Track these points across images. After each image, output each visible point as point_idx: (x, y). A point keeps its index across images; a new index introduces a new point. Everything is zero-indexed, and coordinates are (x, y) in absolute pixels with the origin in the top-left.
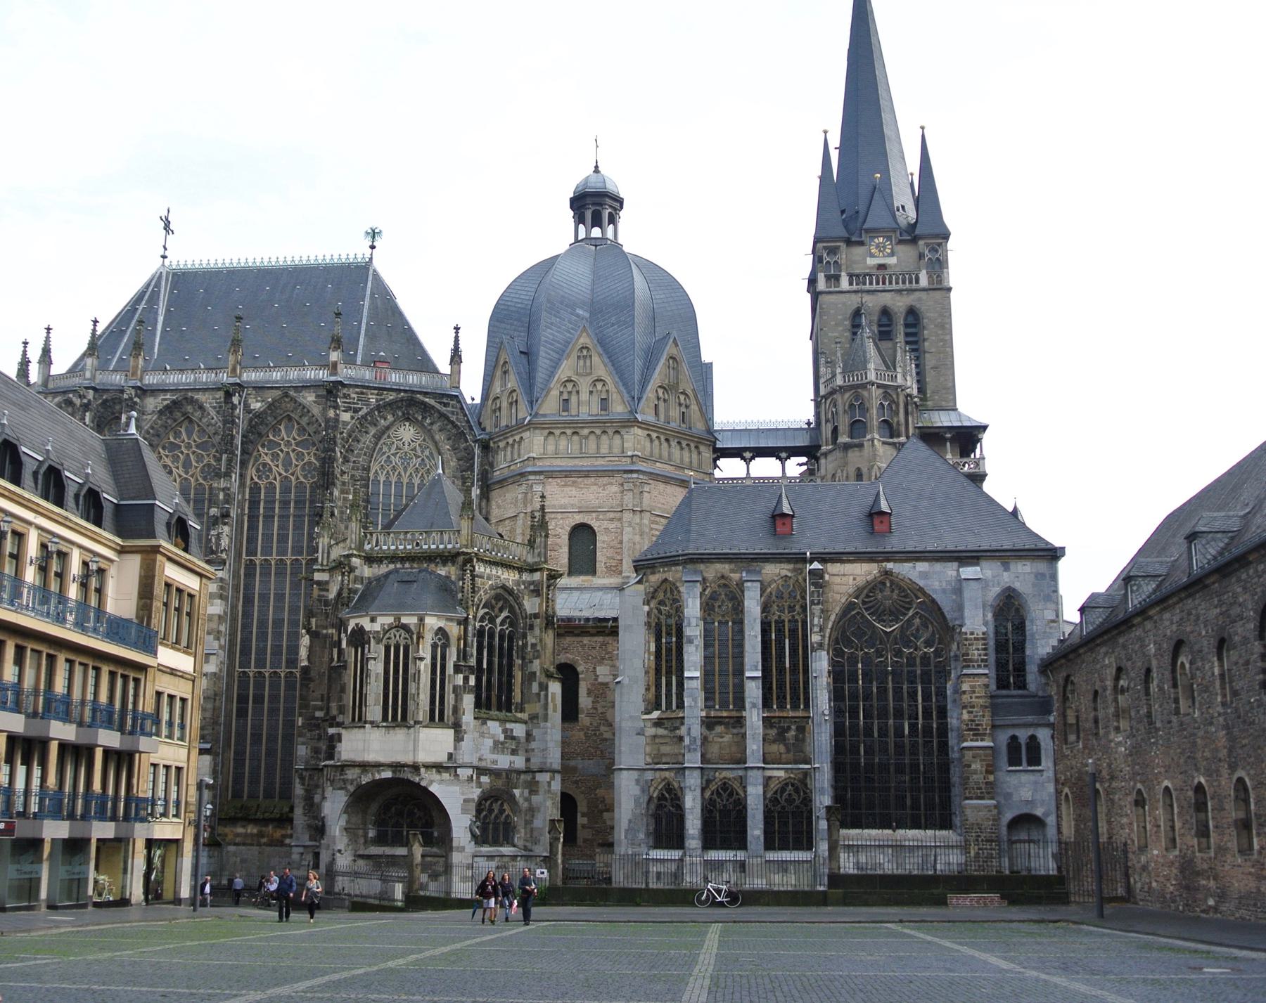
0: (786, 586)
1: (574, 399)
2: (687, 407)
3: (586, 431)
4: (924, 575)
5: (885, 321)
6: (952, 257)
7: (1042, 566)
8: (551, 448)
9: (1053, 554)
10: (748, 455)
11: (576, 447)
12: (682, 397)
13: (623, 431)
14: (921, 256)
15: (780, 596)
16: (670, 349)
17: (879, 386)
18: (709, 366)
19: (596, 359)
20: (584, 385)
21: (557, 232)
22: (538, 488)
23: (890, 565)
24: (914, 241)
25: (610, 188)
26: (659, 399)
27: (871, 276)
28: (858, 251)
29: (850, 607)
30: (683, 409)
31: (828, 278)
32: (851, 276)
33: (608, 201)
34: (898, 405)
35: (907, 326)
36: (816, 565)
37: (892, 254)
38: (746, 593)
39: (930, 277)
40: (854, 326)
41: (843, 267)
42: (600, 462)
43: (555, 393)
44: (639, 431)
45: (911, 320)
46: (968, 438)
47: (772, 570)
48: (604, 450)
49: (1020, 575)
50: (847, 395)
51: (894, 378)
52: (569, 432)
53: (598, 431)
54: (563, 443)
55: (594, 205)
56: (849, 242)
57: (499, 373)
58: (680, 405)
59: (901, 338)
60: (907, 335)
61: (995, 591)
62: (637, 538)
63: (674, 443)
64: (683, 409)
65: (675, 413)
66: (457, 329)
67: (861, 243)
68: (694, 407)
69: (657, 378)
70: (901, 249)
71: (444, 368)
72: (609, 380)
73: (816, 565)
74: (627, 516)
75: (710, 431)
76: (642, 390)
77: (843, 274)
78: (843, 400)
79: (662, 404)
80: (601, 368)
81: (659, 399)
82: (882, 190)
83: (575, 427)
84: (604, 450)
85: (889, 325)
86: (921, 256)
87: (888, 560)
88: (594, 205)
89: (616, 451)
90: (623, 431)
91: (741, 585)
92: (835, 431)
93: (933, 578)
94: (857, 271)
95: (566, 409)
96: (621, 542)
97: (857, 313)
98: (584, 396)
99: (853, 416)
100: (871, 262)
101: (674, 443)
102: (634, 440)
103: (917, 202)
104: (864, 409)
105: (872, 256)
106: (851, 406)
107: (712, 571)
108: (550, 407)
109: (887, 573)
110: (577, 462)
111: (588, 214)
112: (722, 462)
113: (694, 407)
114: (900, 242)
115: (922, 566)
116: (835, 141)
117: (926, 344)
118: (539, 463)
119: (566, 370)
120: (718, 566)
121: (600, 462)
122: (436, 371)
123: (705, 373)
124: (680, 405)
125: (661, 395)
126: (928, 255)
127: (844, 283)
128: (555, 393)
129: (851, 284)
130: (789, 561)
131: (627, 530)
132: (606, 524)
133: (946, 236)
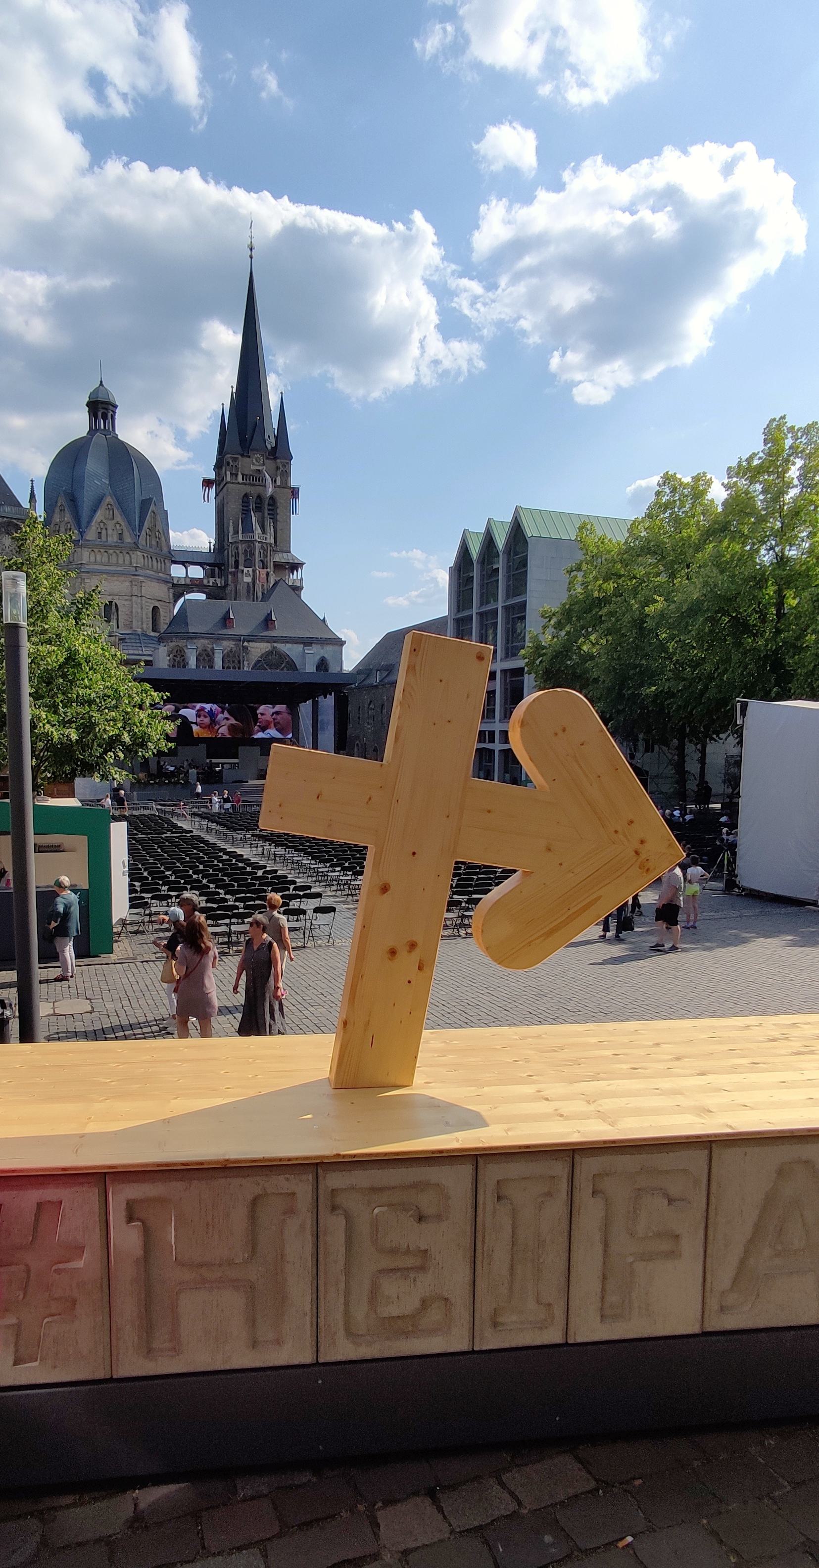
0: (231, 651)
1: (104, 532)
3: (111, 551)
4: (289, 649)
7: (336, 648)
8: (92, 559)
9: (341, 643)
10: (187, 565)
11: (105, 559)
13: (131, 553)
14: (278, 468)
15: (228, 656)
16: (152, 507)
17: (259, 542)
19: (116, 511)
20: (110, 525)
21: (78, 423)
22: (87, 581)
23: (275, 645)
24: (275, 459)
25: (111, 400)
29: (258, 661)
32: (243, 475)
33: (111, 407)
36: (246, 644)
37: (264, 464)
38: (216, 655)
42: (119, 568)
43: (94, 528)
44: (139, 553)
46: (295, 566)
47: (225, 643)
48: (121, 561)
49: (327, 651)
51: (266, 539)
52: (102, 551)
53: (118, 552)
54: (99, 557)
55: (101, 409)
56: (242, 455)
57: (57, 510)
59: (266, 512)
60: (269, 510)
61: (318, 657)
62: (139, 610)
63: (154, 559)
65: (154, 543)
66: (32, 481)
67: (249, 457)
68: (163, 539)
69: (146, 524)
70: (267, 461)
71: (26, 504)
72: (122, 523)
73: (246, 644)
74: (134, 598)
75: (170, 553)
76: (140, 531)
78: (242, 548)
80: (119, 518)
82: (259, 426)
83: (106, 547)
84: (121, 561)
86: (278, 468)
87: (275, 642)
88: (101, 409)
89: (127, 562)
90: (131, 553)
91: (213, 650)
92: (237, 562)
93: (292, 651)
94: (246, 473)
95: (100, 538)
96: (132, 612)
97: (246, 496)
98: (110, 532)
99: (246, 556)
100: (252, 467)
101: (154, 559)
102: (137, 558)
103: (276, 438)
104: (252, 554)
105: (254, 464)
107: (202, 643)
108: (91, 535)
109: (274, 648)
110: (107, 568)
111: (100, 414)
112: (173, 566)
113: (163, 539)
114: (267, 458)
115: (289, 646)
116: (234, 391)
118: (87, 567)
119: (99, 516)
120: (202, 641)
121: (119, 568)
122: (20, 505)
126: (281, 468)
128: (94, 528)
130: (233, 640)
131: (134, 606)
132: (124, 602)
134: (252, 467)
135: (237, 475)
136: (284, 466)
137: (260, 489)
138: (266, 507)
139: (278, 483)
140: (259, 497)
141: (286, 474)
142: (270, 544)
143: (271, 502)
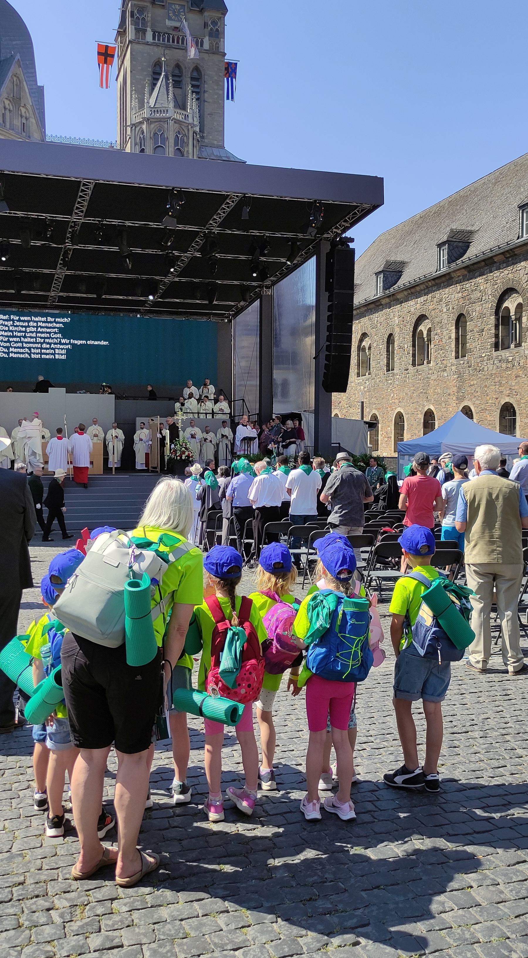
2: (27, 119)
5: (177, 72)
6: (228, 30)
12: (23, 110)
18: (41, 89)
26: (5, 108)
27: (169, 34)
28: (159, 12)
30: (24, 121)
31: (137, 30)
34: (188, 139)
35: (192, 79)
39: (211, 44)
40: (154, 73)
41: (149, 24)
45: (195, 74)
50: (152, 126)
58: (22, 116)
64: (24, 121)
68: (33, 120)
77: (149, 29)
79: (7, 112)
81: (5, 108)
85: (180, 77)
86: (206, 25)
94: (159, 30)
97: (158, 64)
99: (156, 142)
100: (168, 23)
105: (170, 19)
106: (155, 134)
113: (33, 120)
117: (206, 95)
123: (39, 93)
124: (22, 116)
125: (7, 106)
127: (149, 37)
129: (154, 38)
133: (224, 10)
134: (168, 23)
135: (144, 32)
136: (214, 23)
137: (178, 54)
138: (189, 80)
139: (206, 46)
140: (178, 66)
141: (217, 34)
142: (193, 126)
143: (195, 74)
